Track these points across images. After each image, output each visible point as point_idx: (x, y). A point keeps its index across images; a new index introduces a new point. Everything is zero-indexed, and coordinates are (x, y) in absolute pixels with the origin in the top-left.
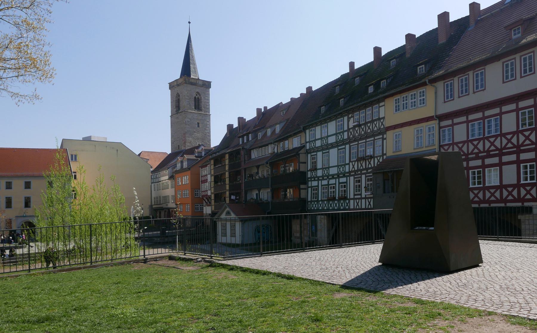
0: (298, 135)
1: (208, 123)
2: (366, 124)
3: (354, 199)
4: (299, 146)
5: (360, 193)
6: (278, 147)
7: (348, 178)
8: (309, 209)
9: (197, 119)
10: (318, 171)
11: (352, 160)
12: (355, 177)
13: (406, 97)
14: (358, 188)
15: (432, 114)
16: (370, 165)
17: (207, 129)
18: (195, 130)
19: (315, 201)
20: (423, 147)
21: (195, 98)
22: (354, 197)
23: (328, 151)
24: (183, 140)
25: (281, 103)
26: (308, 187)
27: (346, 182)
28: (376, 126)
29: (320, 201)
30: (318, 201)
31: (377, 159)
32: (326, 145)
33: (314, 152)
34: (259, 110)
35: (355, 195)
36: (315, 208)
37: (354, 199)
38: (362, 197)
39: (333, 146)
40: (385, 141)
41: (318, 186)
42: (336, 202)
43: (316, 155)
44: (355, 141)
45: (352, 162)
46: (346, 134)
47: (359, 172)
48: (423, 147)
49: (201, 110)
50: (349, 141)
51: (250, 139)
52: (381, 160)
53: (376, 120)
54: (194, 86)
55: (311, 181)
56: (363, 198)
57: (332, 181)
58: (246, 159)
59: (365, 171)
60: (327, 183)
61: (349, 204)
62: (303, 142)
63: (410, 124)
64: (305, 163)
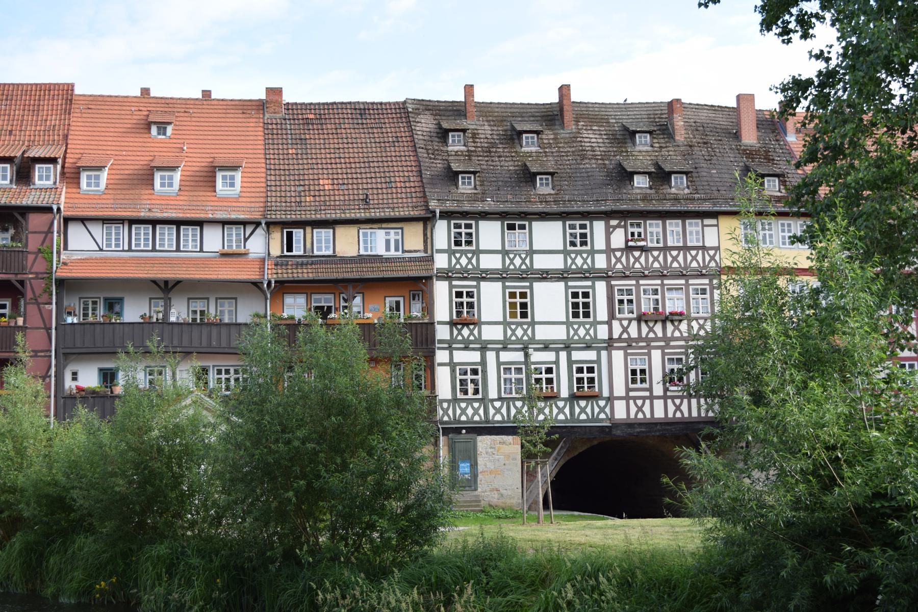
0: (384, 225)
4: (392, 253)
7: (604, 354)
11: (618, 316)
13: (770, 224)
14: (637, 376)
16: (677, 331)
22: (627, 393)
27: (598, 361)
28: (694, 258)
30: (484, 401)
32: (524, 271)
35: (628, 390)
36: (476, 418)
37: (627, 398)
38: (654, 394)
39: (545, 276)
41: (483, 363)
42: (561, 404)
43: (478, 287)
44: (626, 277)
45: (620, 320)
47: (644, 344)
50: (606, 276)
52: (708, 327)
53: (696, 248)
56: (658, 398)
59: (663, 344)
61: (607, 410)
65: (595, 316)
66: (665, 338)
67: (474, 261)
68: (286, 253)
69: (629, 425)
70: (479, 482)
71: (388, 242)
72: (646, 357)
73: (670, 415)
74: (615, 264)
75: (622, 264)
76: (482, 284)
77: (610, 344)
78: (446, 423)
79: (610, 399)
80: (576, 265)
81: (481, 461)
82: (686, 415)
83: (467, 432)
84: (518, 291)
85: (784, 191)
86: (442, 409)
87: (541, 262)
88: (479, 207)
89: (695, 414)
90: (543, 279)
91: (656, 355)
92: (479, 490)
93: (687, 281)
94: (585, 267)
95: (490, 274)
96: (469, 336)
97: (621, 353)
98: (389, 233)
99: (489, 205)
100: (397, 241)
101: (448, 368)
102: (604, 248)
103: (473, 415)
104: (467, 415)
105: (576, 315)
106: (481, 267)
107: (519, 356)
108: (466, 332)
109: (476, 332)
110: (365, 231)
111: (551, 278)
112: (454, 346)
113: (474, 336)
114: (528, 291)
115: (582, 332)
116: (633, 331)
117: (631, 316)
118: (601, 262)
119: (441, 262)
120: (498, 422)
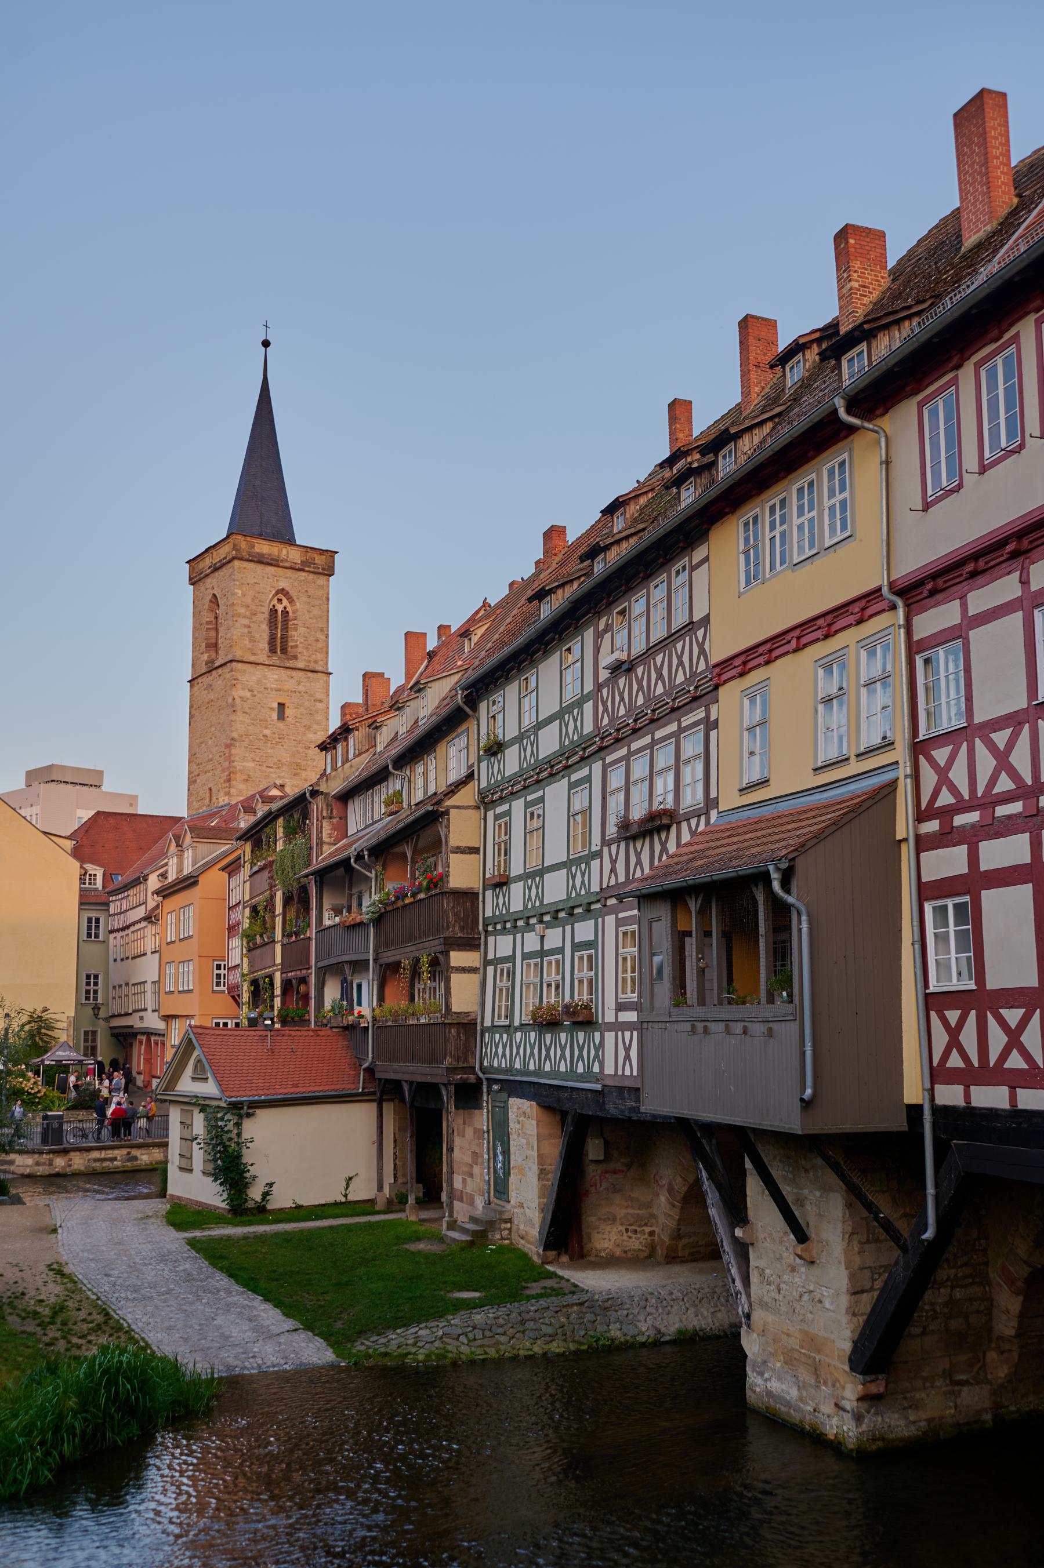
0: (460, 730)
1: (319, 705)
2: (651, 651)
3: (618, 1027)
4: (464, 772)
6: (409, 781)
8: (485, 1064)
9: (280, 690)
10: (513, 886)
12: (621, 915)
13: (783, 502)
15: (875, 578)
17: (315, 727)
18: (267, 732)
20: (848, 759)
21: (273, 611)
23: (540, 793)
24: (223, 771)
26: (487, 963)
29: (516, 1029)
34: (413, 639)
35: (621, 1007)
36: (503, 1066)
37: (618, 1027)
40: (713, 734)
41: (512, 959)
42: (563, 1036)
43: (508, 813)
46: (588, 707)
48: (848, 759)
49: (295, 657)
51: (351, 756)
54: (270, 570)
55: (495, 933)
57: (554, 938)
58: (325, 838)
62: (473, 759)
63: (798, 638)
64: (474, 850)
92: (512, 1202)
120: (519, 1072)
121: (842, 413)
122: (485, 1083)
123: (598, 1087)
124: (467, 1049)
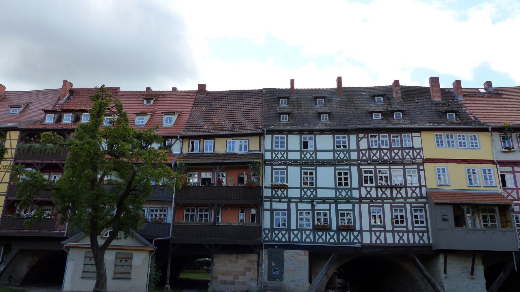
0: (240, 138)
4: (243, 152)
5: (382, 224)
7: (357, 206)
10: (289, 190)
11: (364, 185)
12: (371, 205)
13: (451, 136)
19: (284, 230)
22: (370, 228)
23: (314, 168)
25: (119, 88)
27: (353, 210)
28: (408, 154)
30: (289, 230)
31: (412, 190)
32: (312, 161)
33: (280, 165)
36: (284, 240)
37: (370, 231)
38: (387, 229)
39: (324, 163)
40: (422, 173)
41: (289, 209)
42: (332, 233)
43: (287, 169)
44: (369, 164)
45: (366, 187)
52: (418, 191)
53: (409, 149)
56: (389, 231)
59: (391, 201)
60: (310, 208)
61: (359, 238)
65: (351, 185)
66: (392, 198)
67: (285, 155)
68: (190, 152)
69: (371, 247)
70: (284, 276)
71: (241, 146)
72: (381, 208)
73: (397, 242)
74: (362, 157)
75: (366, 157)
76: (289, 167)
77: (360, 200)
78: (267, 241)
79: (361, 231)
80: (340, 157)
81: (286, 264)
82: (406, 242)
83: (278, 248)
84: (308, 171)
85: (459, 120)
86: (265, 234)
87: (321, 156)
88: (289, 128)
89: (411, 242)
90: (323, 165)
91: (387, 207)
92: (284, 281)
93: (404, 166)
94: (345, 158)
95: (293, 162)
96: (281, 195)
97: (366, 206)
98: (242, 142)
99: (294, 127)
100: (245, 146)
101: (269, 212)
102: (356, 148)
103: (282, 238)
104: (278, 238)
105: (340, 184)
106: (289, 158)
107: (309, 206)
108: (279, 193)
109: (285, 193)
110: (230, 141)
111: (327, 164)
112: (273, 200)
113: (284, 194)
114: (314, 171)
115: (344, 193)
116: (373, 193)
117: (372, 185)
118: (354, 156)
119: (268, 156)
120: (296, 242)
121: (490, 129)
122: (264, 246)
123: (359, 245)
124: (260, 235)
